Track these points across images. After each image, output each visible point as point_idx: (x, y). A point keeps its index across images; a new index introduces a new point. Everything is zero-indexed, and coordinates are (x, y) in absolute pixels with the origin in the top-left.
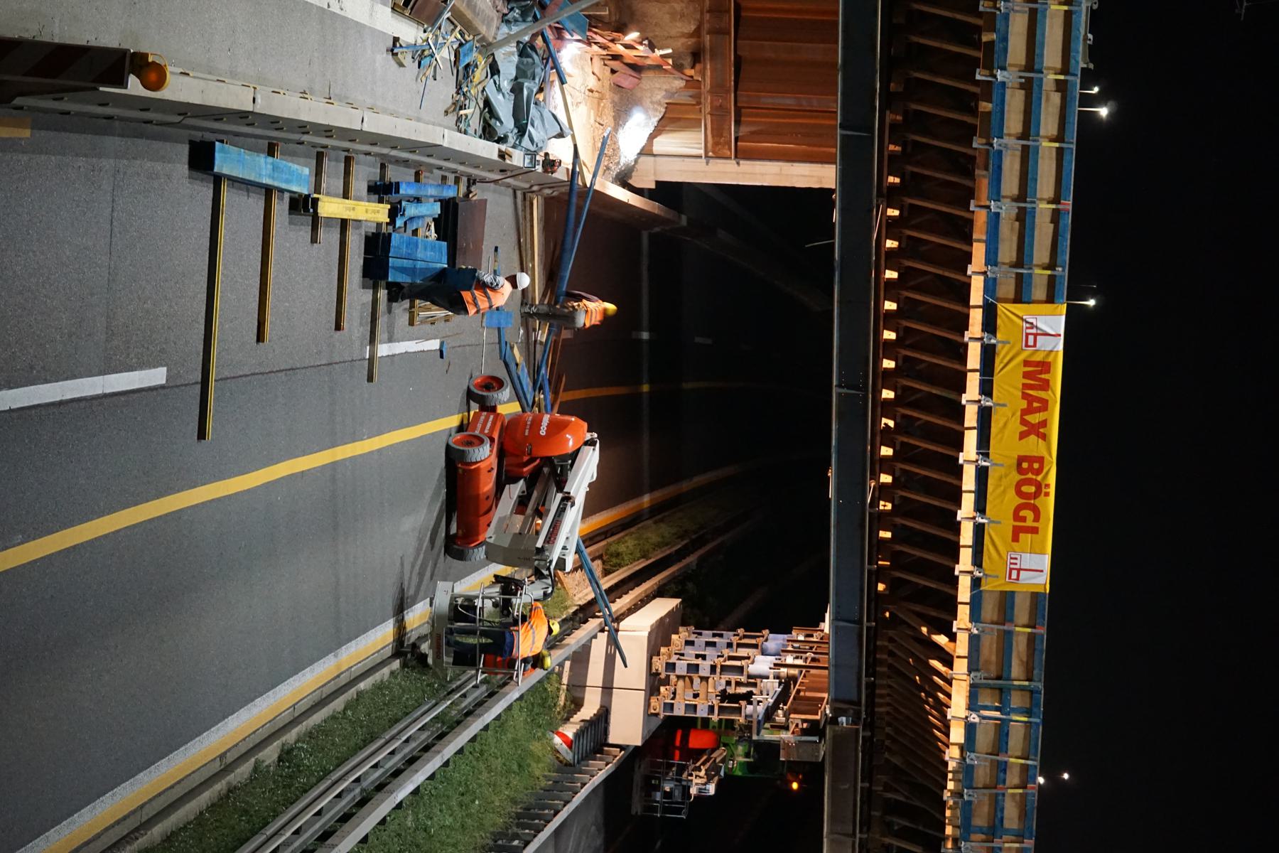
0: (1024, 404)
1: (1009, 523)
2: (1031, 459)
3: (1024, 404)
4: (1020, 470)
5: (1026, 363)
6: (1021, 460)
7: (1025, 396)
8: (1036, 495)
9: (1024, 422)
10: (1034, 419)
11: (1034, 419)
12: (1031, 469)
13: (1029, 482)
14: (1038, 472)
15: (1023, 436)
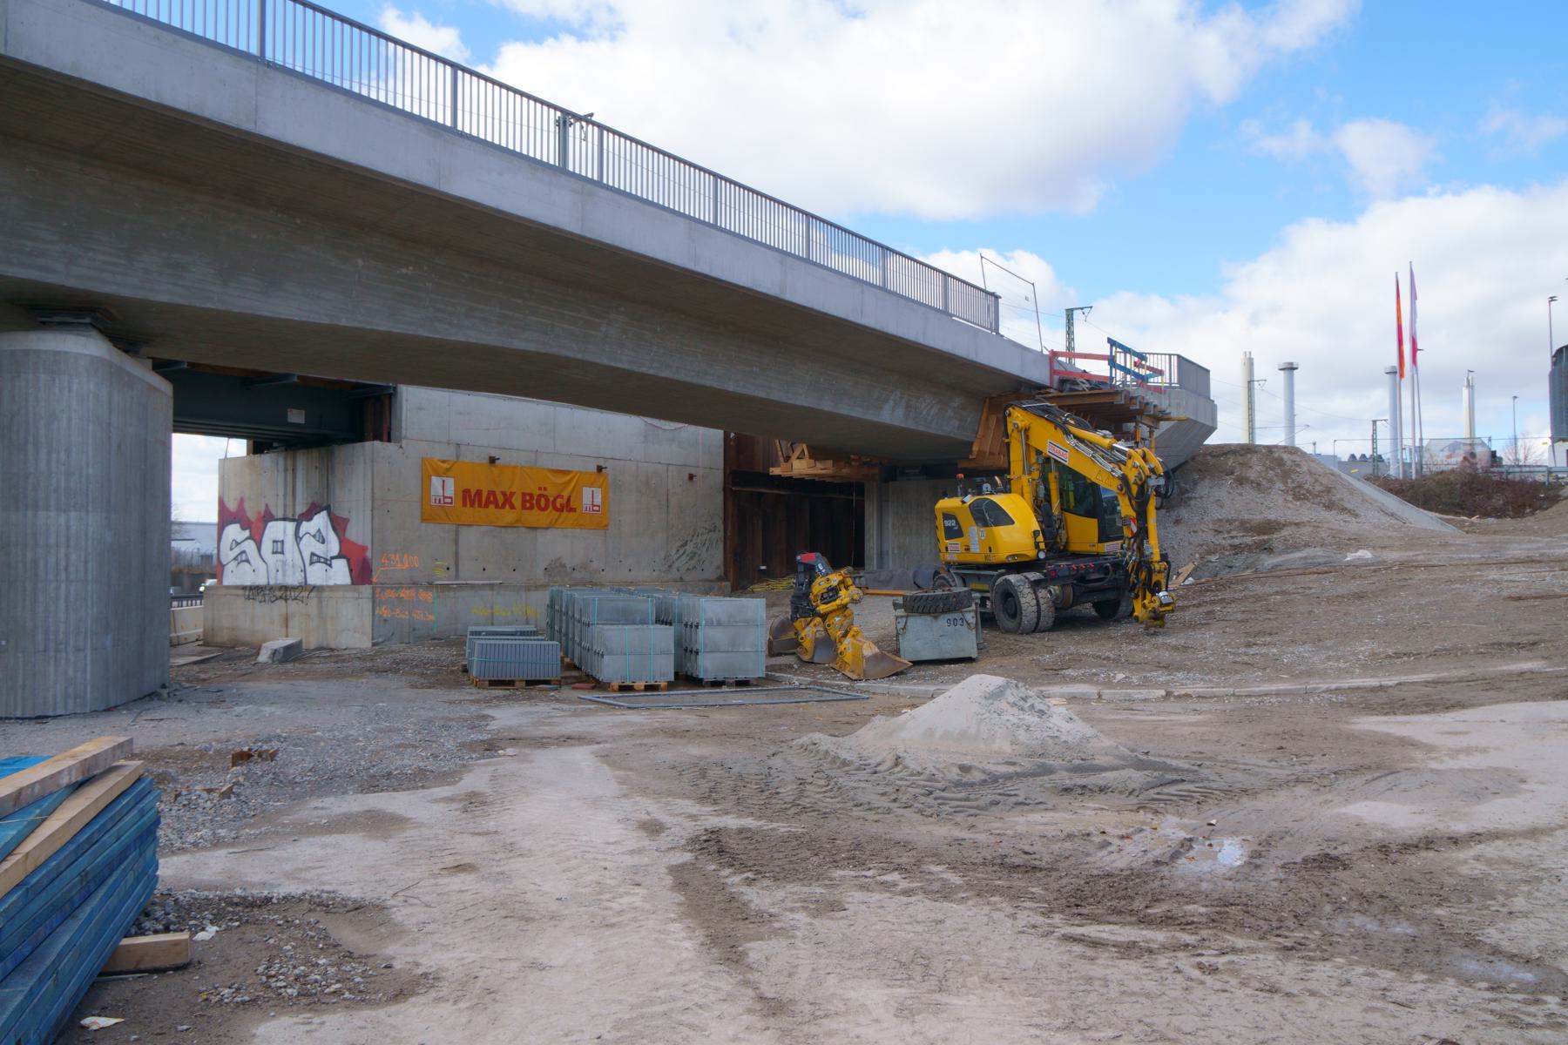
0: (492, 507)
1: (565, 513)
2: (524, 502)
3: (492, 507)
4: (531, 508)
5: (464, 505)
6: (524, 507)
7: (486, 506)
8: (546, 497)
9: (503, 506)
10: (501, 499)
11: (501, 499)
12: (530, 501)
13: (538, 502)
14: (531, 495)
15: (512, 507)
